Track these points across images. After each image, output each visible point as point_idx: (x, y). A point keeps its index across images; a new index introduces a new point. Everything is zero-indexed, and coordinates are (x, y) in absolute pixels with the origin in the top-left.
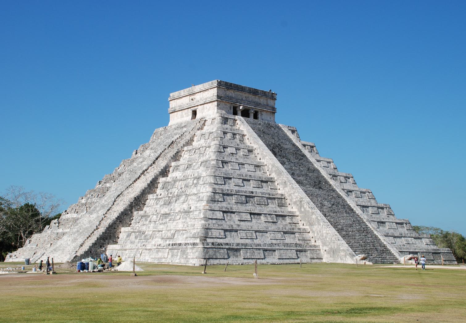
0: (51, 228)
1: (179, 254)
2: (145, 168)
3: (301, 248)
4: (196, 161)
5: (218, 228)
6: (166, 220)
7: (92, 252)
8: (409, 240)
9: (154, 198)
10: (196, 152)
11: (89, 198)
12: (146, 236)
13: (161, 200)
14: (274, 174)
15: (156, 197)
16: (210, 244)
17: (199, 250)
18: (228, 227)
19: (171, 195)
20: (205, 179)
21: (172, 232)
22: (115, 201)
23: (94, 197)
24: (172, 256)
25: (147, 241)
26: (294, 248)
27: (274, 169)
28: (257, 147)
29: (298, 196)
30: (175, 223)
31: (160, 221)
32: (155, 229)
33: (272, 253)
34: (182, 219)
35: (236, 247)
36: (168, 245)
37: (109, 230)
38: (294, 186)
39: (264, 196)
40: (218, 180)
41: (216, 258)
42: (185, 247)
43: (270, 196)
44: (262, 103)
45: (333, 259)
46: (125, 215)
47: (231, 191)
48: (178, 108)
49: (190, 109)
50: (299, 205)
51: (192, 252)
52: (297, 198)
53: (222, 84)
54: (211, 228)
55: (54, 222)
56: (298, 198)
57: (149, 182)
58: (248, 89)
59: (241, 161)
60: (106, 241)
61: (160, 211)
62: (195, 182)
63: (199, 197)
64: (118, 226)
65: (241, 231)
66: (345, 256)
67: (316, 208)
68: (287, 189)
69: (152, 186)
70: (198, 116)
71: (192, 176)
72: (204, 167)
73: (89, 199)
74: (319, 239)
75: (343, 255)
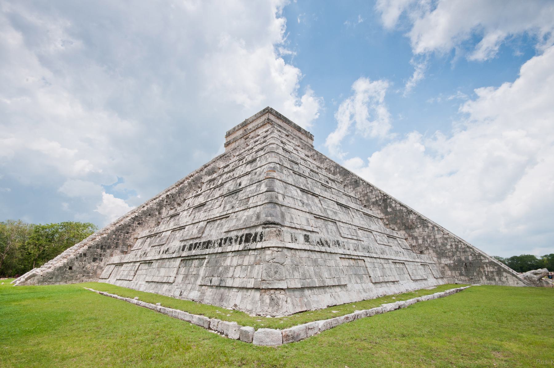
7: (74, 268)
14: (338, 175)
16: (301, 239)
17: (267, 258)
27: (338, 170)
29: (380, 194)
35: (355, 253)
37: (116, 235)
41: (322, 285)
45: (467, 278)
46: (150, 215)
51: (241, 265)
52: (377, 196)
54: (289, 205)
60: (108, 251)
64: (134, 230)
65: (341, 224)
68: (359, 189)
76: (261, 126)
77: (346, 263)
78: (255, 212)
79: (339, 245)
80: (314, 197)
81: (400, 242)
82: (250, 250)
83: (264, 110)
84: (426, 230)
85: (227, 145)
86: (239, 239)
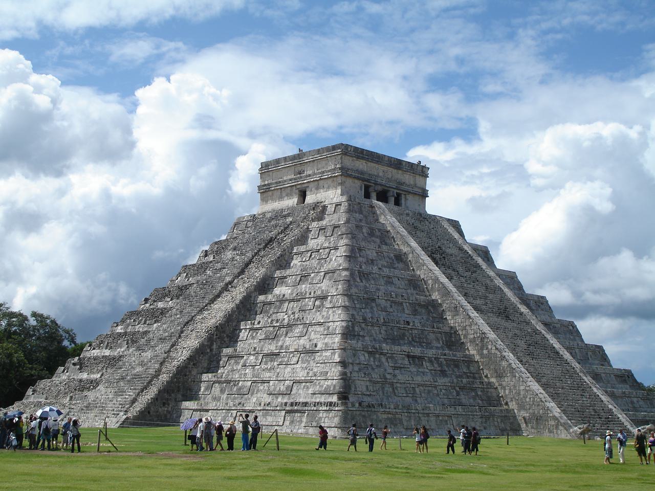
0: (67, 372)
1: (304, 420)
2: (228, 279)
3: (488, 414)
4: (316, 271)
5: (365, 379)
7: (151, 413)
8: (635, 402)
9: (248, 327)
10: (313, 257)
11: (128, 325)
12: (240, 389)
13: (260, 331)
14: (437, 293)
15: (251, 327)
16: (357, 405)
18: (379, 377)
19: (278, 324)
20: (335, 300)
22: (182, 332)
23: (139, 324)
24: (292, 422)
25: (242, 398)
26: (478, 414)
27: (437, 287)
29: (478, 330)
30: (289, 369)
31: (263, 366)
33: (446, 421)
34: (302, 363)
36: (283, 404)
37: (176, 378)
38: (472, 315)
39: (426, 329)
40: (356, 302)
43: (434, 330)
44: (407, 182)
46: (202, 353)
47: (378, 320)
50: (480, 345)
55: (73, 362)
56: (478, 334)
57: (238, 302)
58: (386, 159)
59: (386, 271)
61: (262, 348)
62: (317, 303)
64: (190, 372)
65: (399, 385)
66: (557, 428)
67: (507, 350)
68: (459, 319)
69: (246, 309)
70: (310, 199)
71: (312, 294)
72: (330, 280)
73: (130, 327)
75: (553, 426)
77: (385, 416)
78: (332, 383)
79: (382, 406)
80: (382, 356)
81: (479, 393)
82: (332, 410)
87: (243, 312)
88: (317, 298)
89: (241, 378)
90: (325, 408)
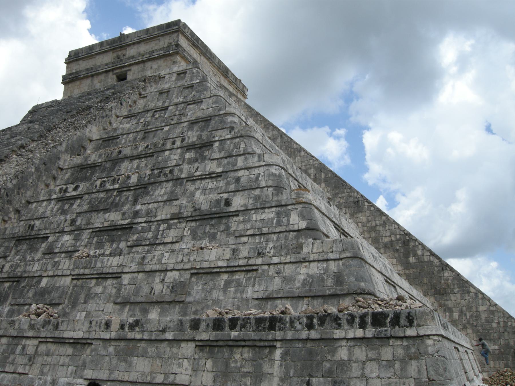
4: (172, 122)
6: (114, 246)
13: (79, 201)
15: (60, 195)
19: (117, 186)
21: (171, 276)
27: (323, 176)
28: (274, 135)
29: (398, 231)
32: (85, 268)
34: (194, 239)
42: (314, 334)
48: (85, 73)
49: (111, 73)
50: (402, 250)
51: (377, 360)
52: (392, 234)
53: (186, 31)
56: (398, 236)
58: (217, 61)
61: (89, 220)
63: (238, 180)
68: (363, 217)
74: (467, 326)
76: (160, 57)
78: (326, 270)
82: (392, 337)
83: (169, 25)
84: (467, 297)
85: (67, 80)
86: (357, 320)
87: (44, 178)
88: (189, 148)
89: (46, 270)
90: (360, 333)
